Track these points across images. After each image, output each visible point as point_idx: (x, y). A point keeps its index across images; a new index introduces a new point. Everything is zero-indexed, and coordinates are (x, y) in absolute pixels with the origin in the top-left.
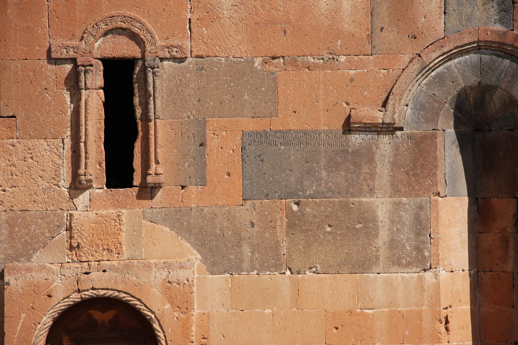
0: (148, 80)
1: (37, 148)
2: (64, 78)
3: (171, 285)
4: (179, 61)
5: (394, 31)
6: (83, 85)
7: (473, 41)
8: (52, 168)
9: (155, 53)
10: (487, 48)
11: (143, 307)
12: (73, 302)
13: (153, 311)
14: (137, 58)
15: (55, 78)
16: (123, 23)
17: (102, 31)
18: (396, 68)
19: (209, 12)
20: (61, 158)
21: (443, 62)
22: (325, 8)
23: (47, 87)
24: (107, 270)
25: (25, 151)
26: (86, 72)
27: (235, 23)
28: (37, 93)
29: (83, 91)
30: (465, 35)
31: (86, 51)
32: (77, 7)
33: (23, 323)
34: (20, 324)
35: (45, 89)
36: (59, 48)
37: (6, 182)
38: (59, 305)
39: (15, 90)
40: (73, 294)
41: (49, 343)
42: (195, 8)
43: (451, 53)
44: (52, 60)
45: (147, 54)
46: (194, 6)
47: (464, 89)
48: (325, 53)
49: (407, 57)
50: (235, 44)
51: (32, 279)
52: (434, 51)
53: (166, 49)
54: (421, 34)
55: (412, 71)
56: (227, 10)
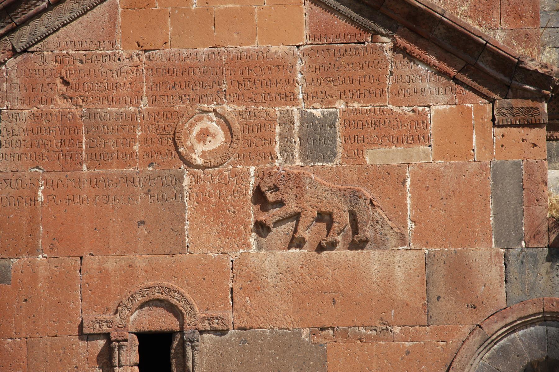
0: (187, 355)
2: (96, 355)
4: (220, 334)
5: (452, 300)
6: (117, 362)
7: (538, 312)
9: (194, 325)
10: (553, 319)
14: (175, 331)
15: (86, 355)
16: (160, 294)
17: (138, 303)
18: (455, 340)
19: (252, 281)
21: (506, 334)
22: (377, 276)
23: (77, 366)
26: (120, 347)
27: (281, 292)
29: (117, 368)
30: (528, 306)
31: (121, 325)
32: (112, 278)
36: (91, 322)
42: (238, 277)
43: (515, 324)
44: (84, 336)
45: (186, 326)
46: (236, 274)
47: (531, 364)
48: (377, 323)
49: (467, 329)
50: (280, 314)
52: (496, 322)
53: (206, 321)
54: (481, 303)
55: (473, 343)
56: (272, 278)
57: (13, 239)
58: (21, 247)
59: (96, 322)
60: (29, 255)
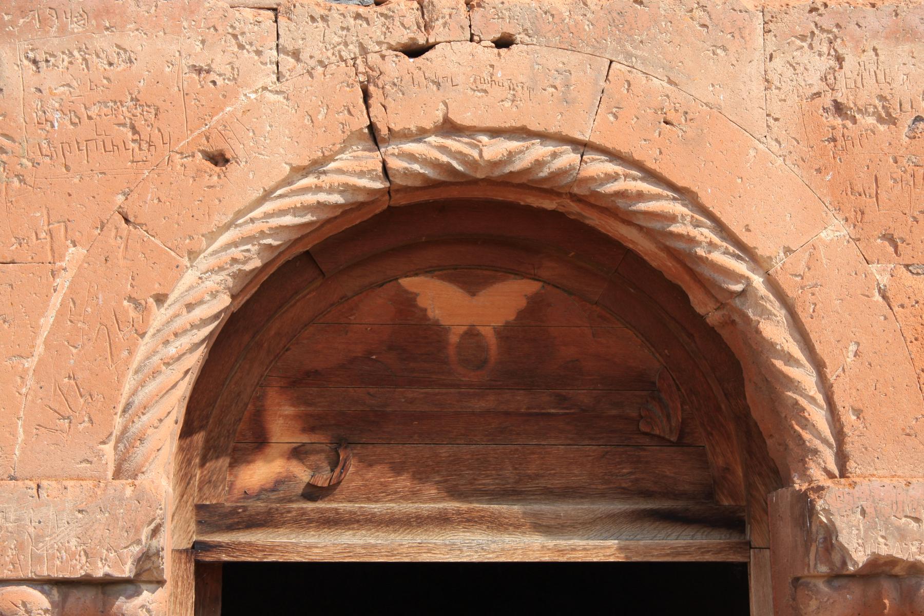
3: (849, 124)
11: (706, 231)
12: (341, 193)
13: (760, 252)
24: (518, 38)
33: (72, 297)
34: (56, 300)
38: (268, 207)
40: (342, 151)
41: (201, 428)
51: (123, 66)
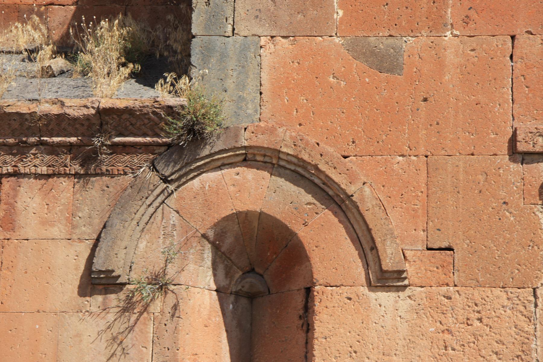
1: (489, 303)
8: (515, 339)
15: (521, 185)
20: (532, 321)
23: (507, 201)
25: (469, 307)
28: (490, 209)
35: (505, 203)
36: (530, 135)
37: (435, 360)
39: (452, 205)
44: (517, 156)
57: (407, 8)
58: (418, 20)
59: (537, 134)
60: (431, 32)
